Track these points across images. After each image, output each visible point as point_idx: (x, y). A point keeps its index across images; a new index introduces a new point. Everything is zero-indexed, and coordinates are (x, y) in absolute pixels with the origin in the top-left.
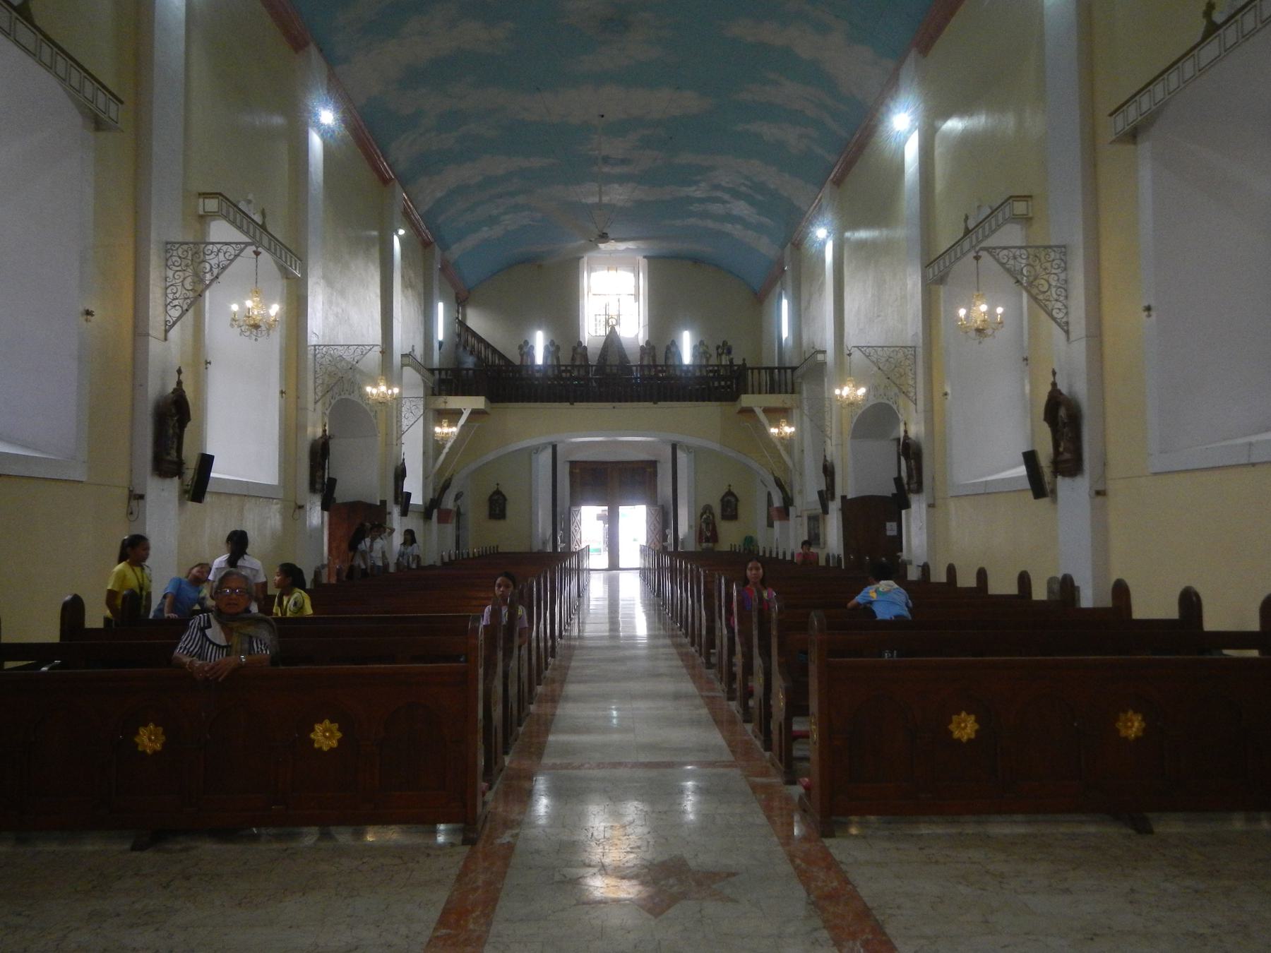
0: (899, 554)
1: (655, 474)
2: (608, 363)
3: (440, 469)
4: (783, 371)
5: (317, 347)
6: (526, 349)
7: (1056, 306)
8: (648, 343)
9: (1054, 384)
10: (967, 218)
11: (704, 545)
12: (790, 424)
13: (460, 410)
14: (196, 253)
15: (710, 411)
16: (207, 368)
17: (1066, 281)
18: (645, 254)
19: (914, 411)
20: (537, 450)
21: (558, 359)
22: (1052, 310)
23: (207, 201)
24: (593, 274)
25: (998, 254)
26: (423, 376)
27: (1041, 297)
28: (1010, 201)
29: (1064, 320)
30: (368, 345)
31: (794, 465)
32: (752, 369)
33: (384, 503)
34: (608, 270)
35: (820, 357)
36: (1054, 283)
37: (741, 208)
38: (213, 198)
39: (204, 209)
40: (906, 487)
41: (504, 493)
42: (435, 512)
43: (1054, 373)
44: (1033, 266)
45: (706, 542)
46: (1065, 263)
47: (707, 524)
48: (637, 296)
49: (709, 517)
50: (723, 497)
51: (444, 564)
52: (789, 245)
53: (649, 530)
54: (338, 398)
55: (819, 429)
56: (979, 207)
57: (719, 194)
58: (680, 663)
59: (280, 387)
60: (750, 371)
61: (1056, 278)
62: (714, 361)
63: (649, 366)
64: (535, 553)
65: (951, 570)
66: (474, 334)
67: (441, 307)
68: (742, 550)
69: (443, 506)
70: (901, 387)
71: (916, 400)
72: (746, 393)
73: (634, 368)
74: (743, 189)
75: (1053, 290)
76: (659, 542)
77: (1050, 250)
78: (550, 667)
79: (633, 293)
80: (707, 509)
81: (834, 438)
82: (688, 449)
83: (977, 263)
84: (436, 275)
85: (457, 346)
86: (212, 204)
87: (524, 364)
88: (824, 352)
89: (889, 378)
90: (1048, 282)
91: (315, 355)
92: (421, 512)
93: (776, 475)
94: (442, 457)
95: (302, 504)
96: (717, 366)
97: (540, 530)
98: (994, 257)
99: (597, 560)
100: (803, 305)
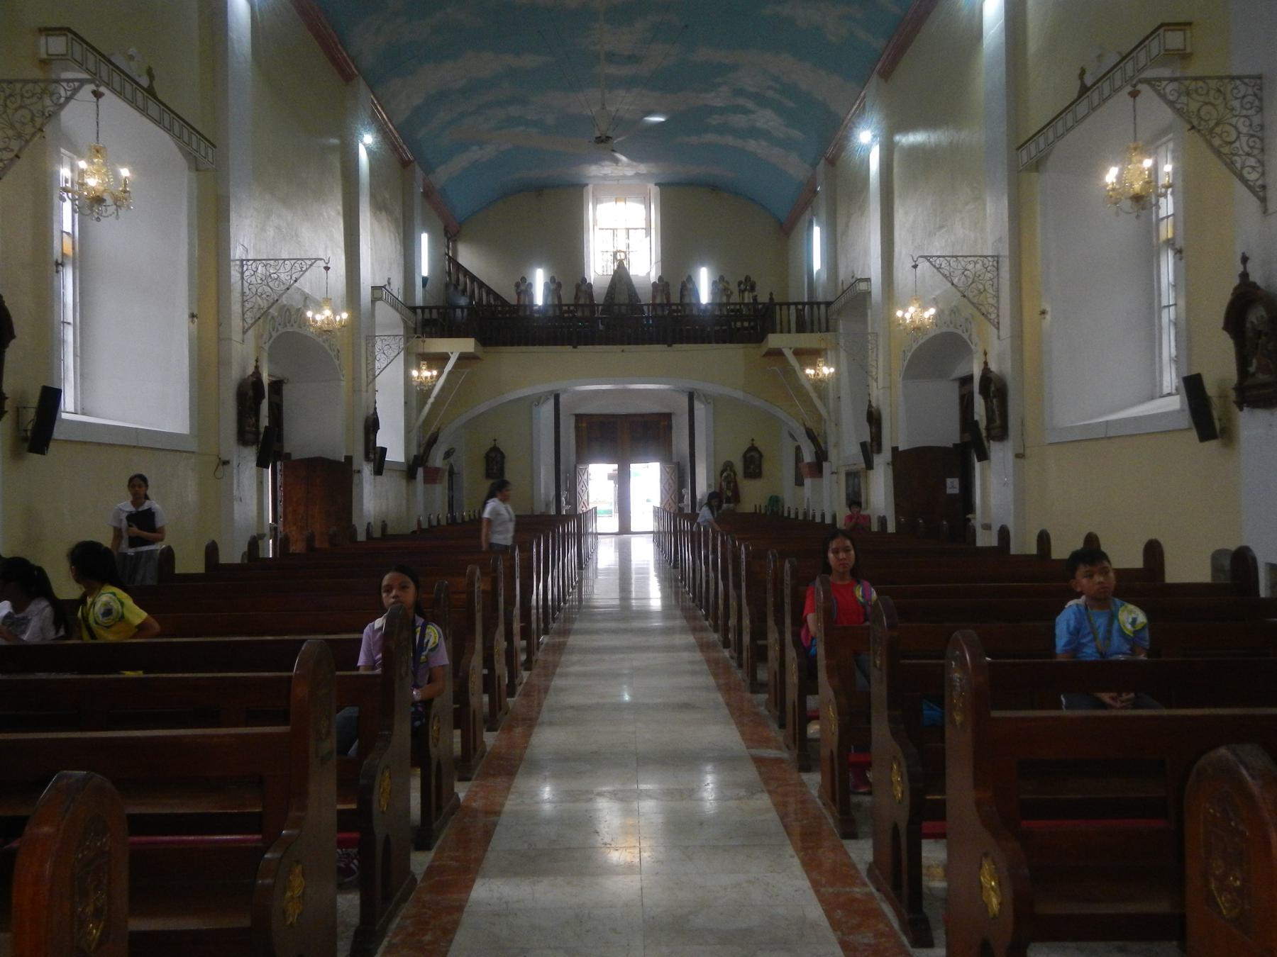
0: (970, 516)
1: (669, 427)
2: (617, 302)
3: (425, 421)
4: (815, 307)
5: (245, 262)
6: (524, 288)
7: (1248, 163)
8: (660, 279)
9: (1244, 275)
10: (1083, 72)
12: (827, 364)
13: (447, 354)
14: (11, 95)
15: (733, 355)
16: (57, 272)
17: (1262, 127)
19: (996, 337)
20: (538, 400)
21: (559, 298)
22: (1242, 168)
23: (50, 39)
24: (599, 207)
25: (1164, 89)
26: (400, 313)
27: (1225, 150)
28: (1161, 31)
29: (1259, 183)
30: (310, 259)
31: (829, 413)
32: (781, 304)
33: (349, 459)
34: (616, 202)
35: (863, 286)
36: (1244, 130)
37: (766, 119)
38: (60, 35)
39: (47, 51)
40: (984, 434)
41: (502, 450)
42: (420, 471)
43: (1245, 260)
44: (1214, 106)
45: (726, 503)
46: (1261, 100)
47: (729, 483)
48: (648, 230)
50: (747, 452)
51: (431, 526)
52: (823, 161)
53: (664, 491)
54: (281, 330)
55: (859, 368)
56: (1100, 57)
57: (740, 101)
58: (711, 681)
59: (190, 308)
60: (778, 307)
61: (1247, 123)
62: (735, 298)
63: (662, 305)
64: (537, 516)
65: (1044, 539)
66: (466, 273)
67: (425, 238)
68: (763, 511)
69: (430, 464)
70: (980, 307)
71: (998, 323)
72: (774, 332)
73: (645, 308)
74: (770, 93)
75: (1244, 139)
77: (1238, 82)
78: (519, 689)
79: (644, 227)
80: (728, 466)
81: (880, 380)
82: (707, 398)
83: (1134, 102)
84: (418, 201)
85: (447, 285)
86: (57, 45)
87: (521, 303)
88: (868, 280)
89: (964, 296)
90: (1236, 127)
91: (242, 273)
92: (403, 471)
93: (807, 426)
95: (227, 459)
96: (740, 304)
97: (542, 491)
98: (1159, 94)
99: (606, 523)
100: (840, 229)
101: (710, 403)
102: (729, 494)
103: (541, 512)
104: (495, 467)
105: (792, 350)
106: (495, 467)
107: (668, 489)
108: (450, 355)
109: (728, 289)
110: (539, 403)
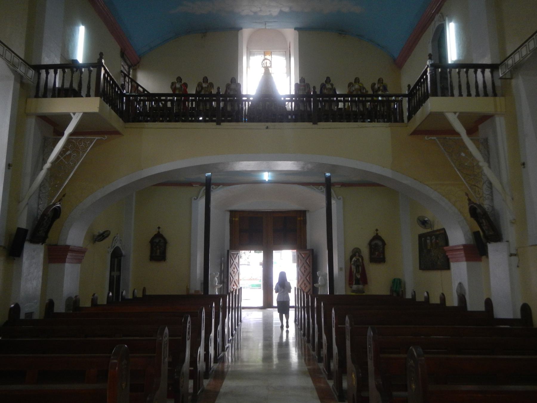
1: (304, 222)
4: (479, 71)
8: (302, 80)
11: (355, 287)
18: (298, 26)
24: (251, 58)
41: (166, 235)
45: (356, 284)
47: (357, 267)
48: (289, 73)
49: (358, 259)
50: (371, 241)
53: (299, 271)
76: (310, 284)
80: (356, 252)
94: (42, 174)
101: (340, 199)
102: (359, 277)
103: (196, 291)
104: (158, 251)
105: (457, 114)
106: (158, 251)
107: (303, 271)
108: (72, 115)
109: (364, 88)
110: (197, 198)
